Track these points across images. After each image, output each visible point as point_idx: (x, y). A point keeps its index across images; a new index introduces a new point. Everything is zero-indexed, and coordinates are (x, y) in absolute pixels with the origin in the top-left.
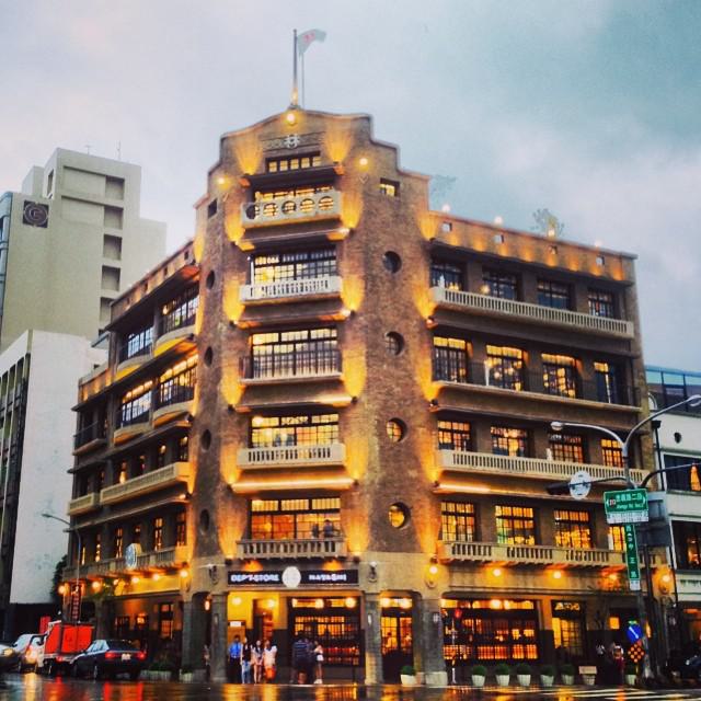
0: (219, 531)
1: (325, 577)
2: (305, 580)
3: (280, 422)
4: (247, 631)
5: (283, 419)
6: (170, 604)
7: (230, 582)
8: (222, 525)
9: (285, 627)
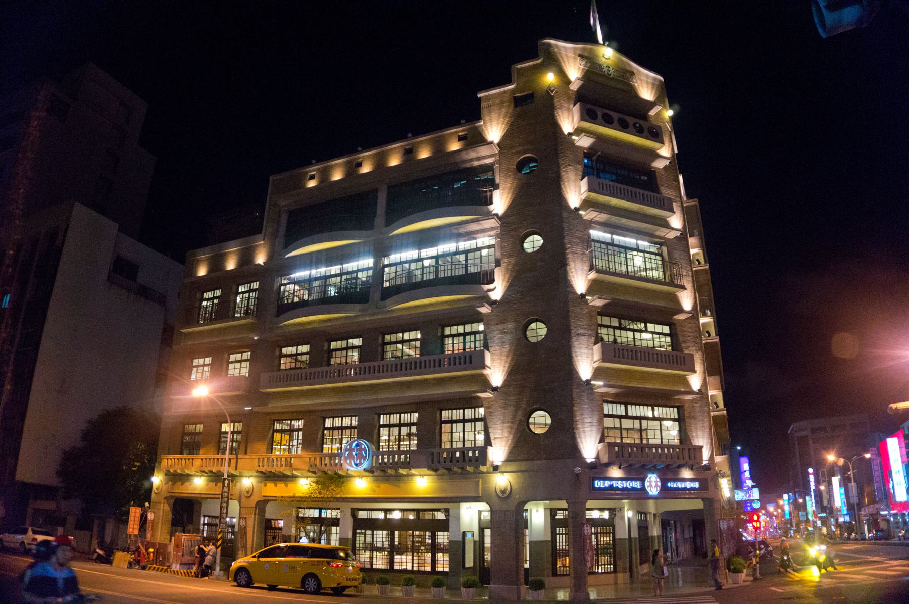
0: (575, 431)
1: (680, 485)
2: (664, 488)
3: (620, 323)
4: (475, 542)
5: (623, 321)
6: (320, 509)
7: (595, 489)
8: (579, 426)
9: (549, 539)
